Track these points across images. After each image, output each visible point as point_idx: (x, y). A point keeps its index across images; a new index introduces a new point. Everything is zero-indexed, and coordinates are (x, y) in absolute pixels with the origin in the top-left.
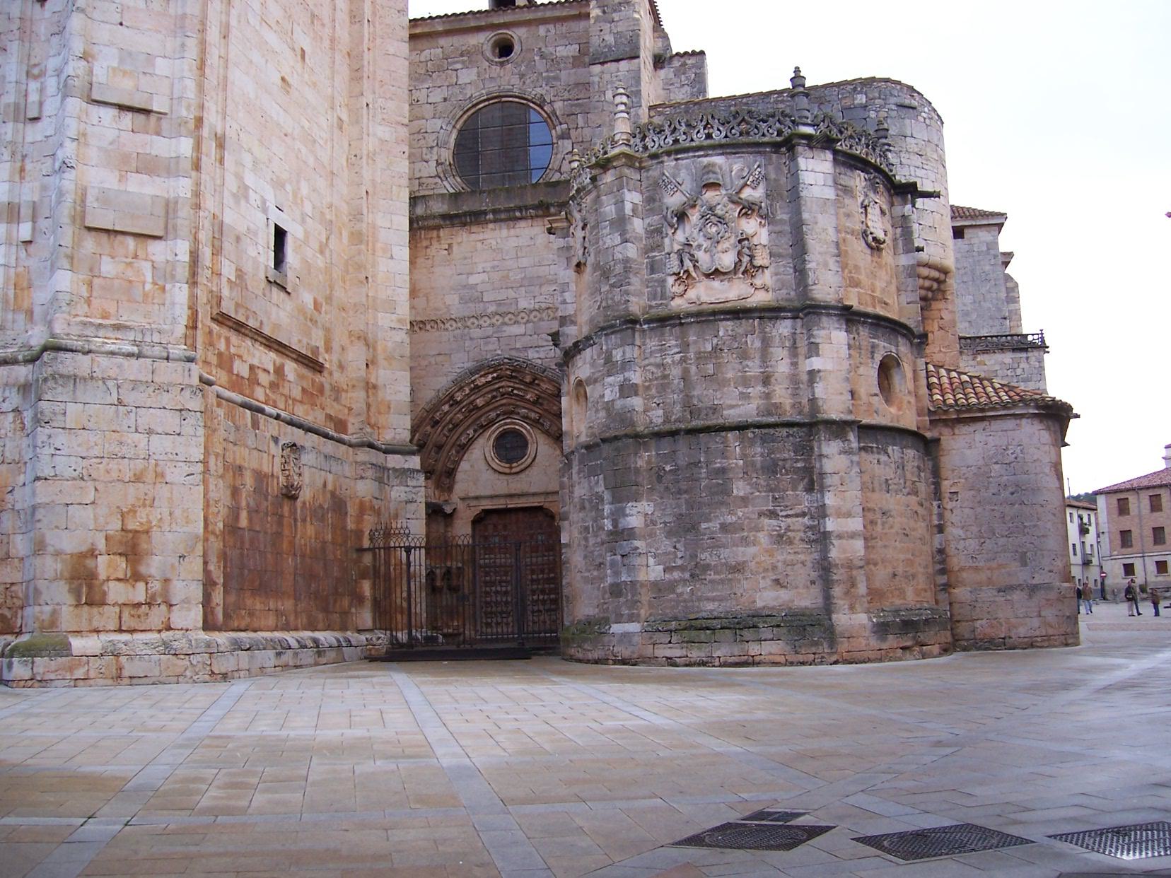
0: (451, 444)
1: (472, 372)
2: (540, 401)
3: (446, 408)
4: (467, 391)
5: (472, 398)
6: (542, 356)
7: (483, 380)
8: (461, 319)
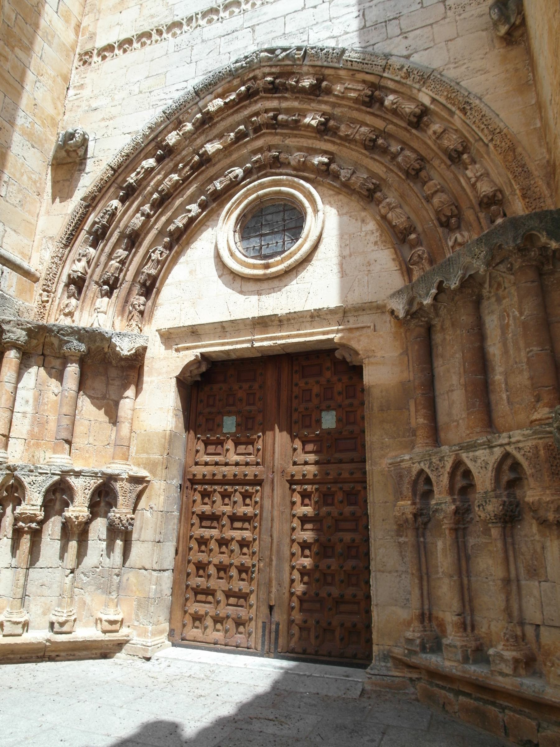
0: (154, 232)
1: (198, 93)
2: (332, 123)
3: (150, 162)
4: (189, 127)
5: (199, 142)
6: (335, 33)
7: (219, 102)
8: (190, 19)
